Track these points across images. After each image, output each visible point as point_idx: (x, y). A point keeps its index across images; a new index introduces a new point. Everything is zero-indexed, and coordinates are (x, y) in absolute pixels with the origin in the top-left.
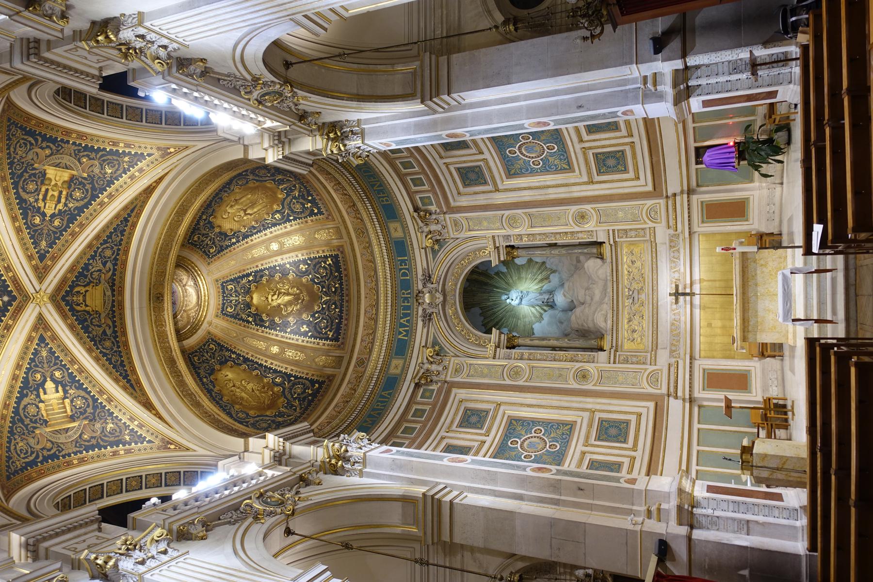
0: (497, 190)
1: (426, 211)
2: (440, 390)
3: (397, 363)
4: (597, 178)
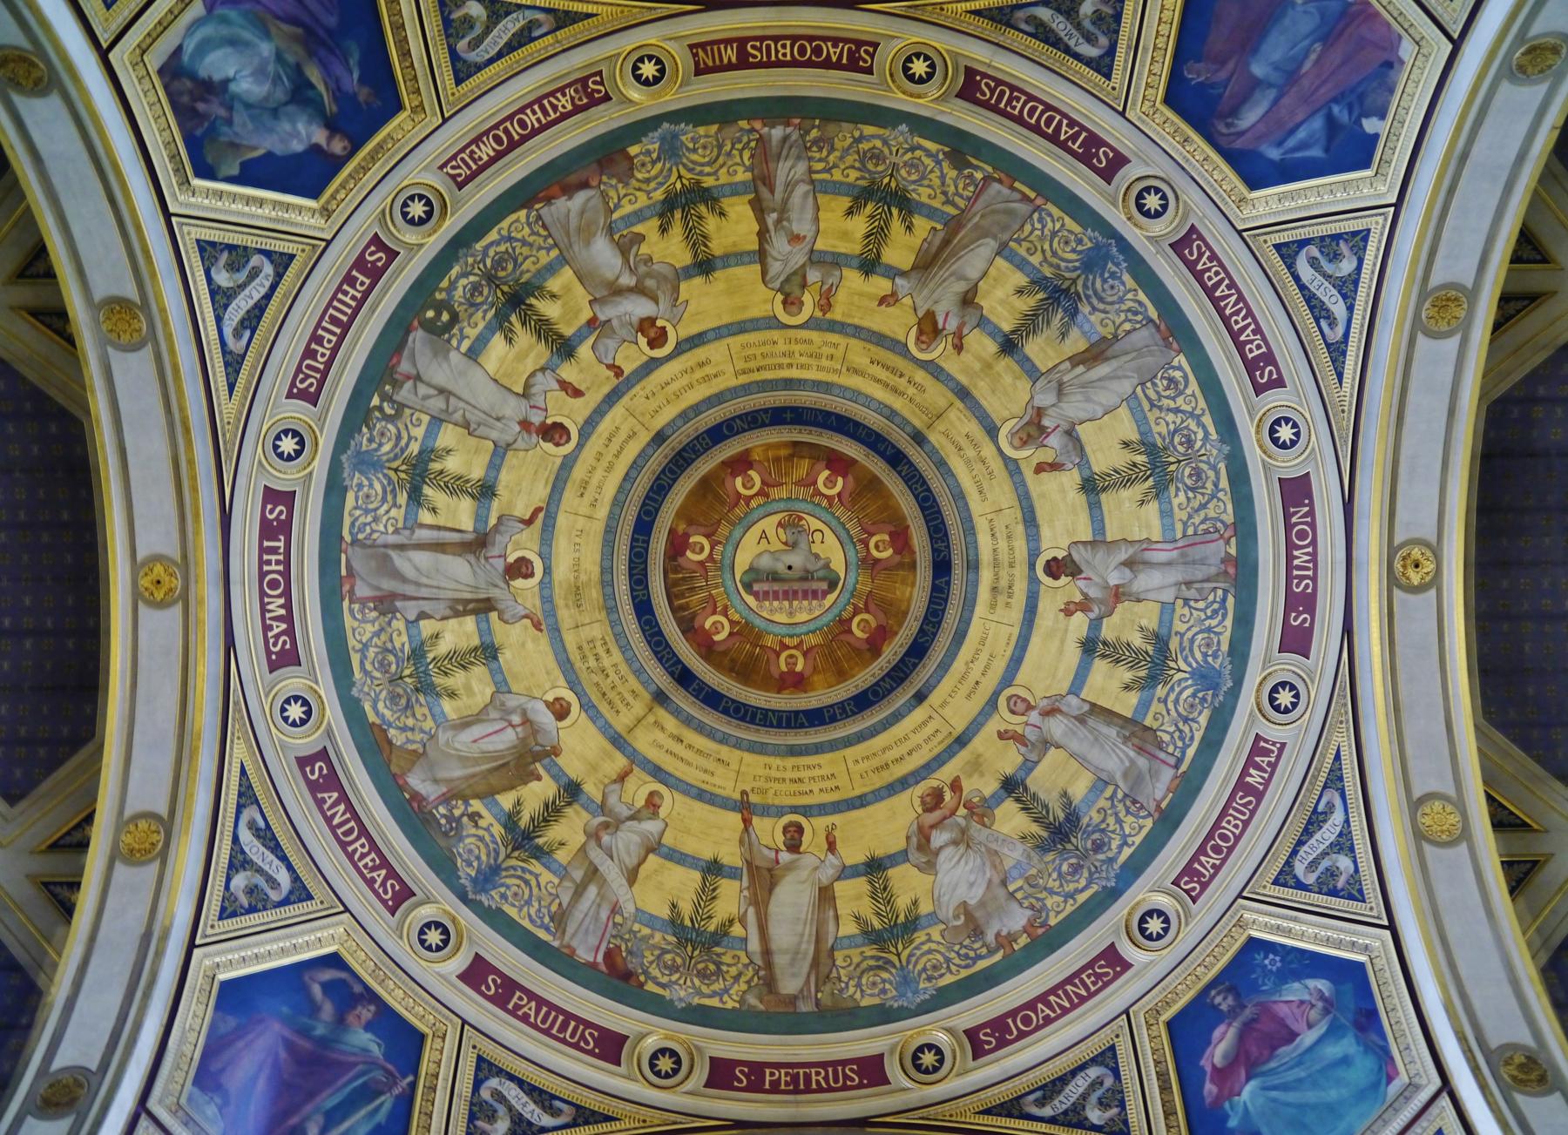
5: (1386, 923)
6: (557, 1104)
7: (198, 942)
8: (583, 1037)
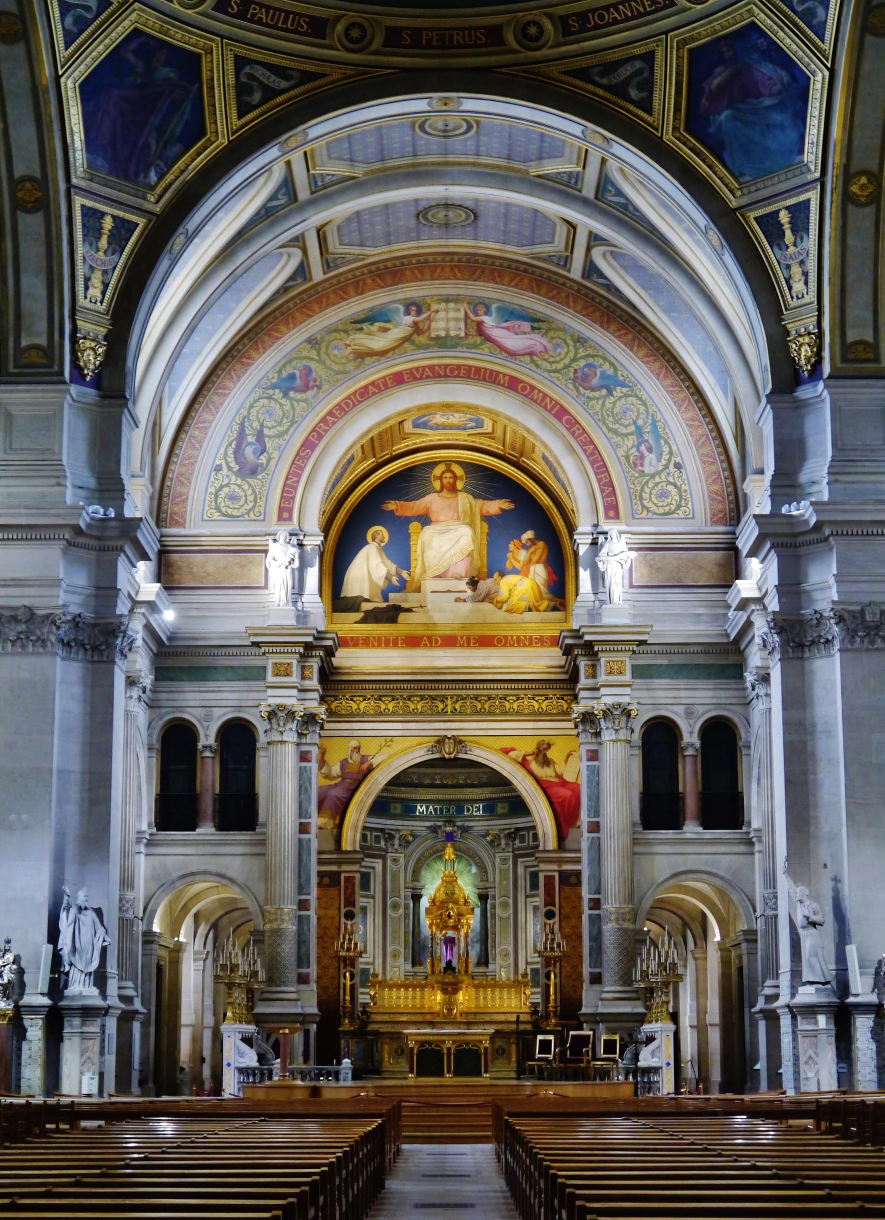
0: (527, 897)
1: (514, 840)
2: (380, 849)
3: (398, 808)
4: (529, 967)
5: (829, 65)
6: (289, 72)
7: (60, 73)
8: (299, 24)
